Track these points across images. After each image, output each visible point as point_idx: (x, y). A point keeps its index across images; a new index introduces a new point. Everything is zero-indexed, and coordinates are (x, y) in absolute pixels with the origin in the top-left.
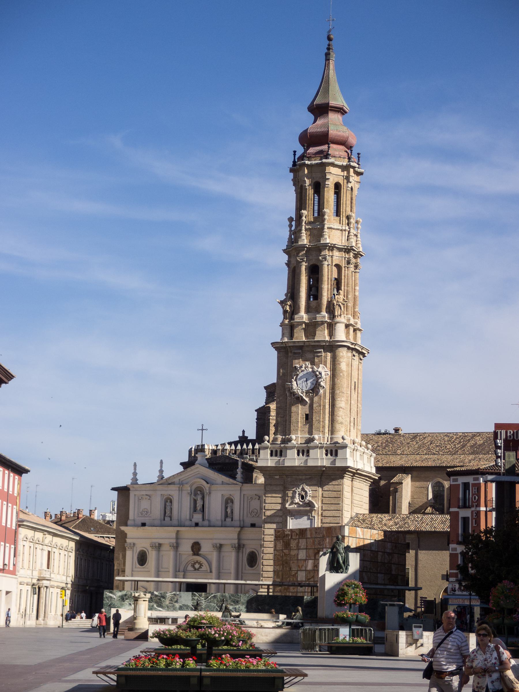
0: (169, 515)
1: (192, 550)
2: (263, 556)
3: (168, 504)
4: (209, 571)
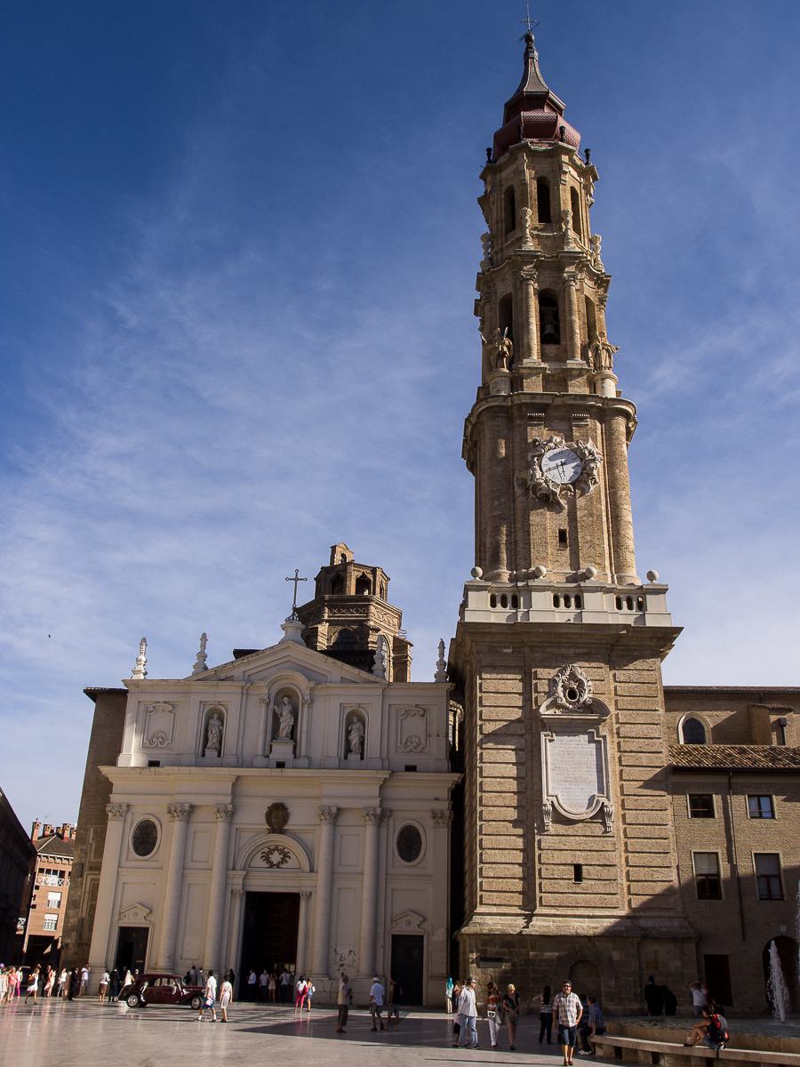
0: (214, 746)
1: (269, 821)
2: (481, 826)
3: (214, 722)
4: (306, 867)
